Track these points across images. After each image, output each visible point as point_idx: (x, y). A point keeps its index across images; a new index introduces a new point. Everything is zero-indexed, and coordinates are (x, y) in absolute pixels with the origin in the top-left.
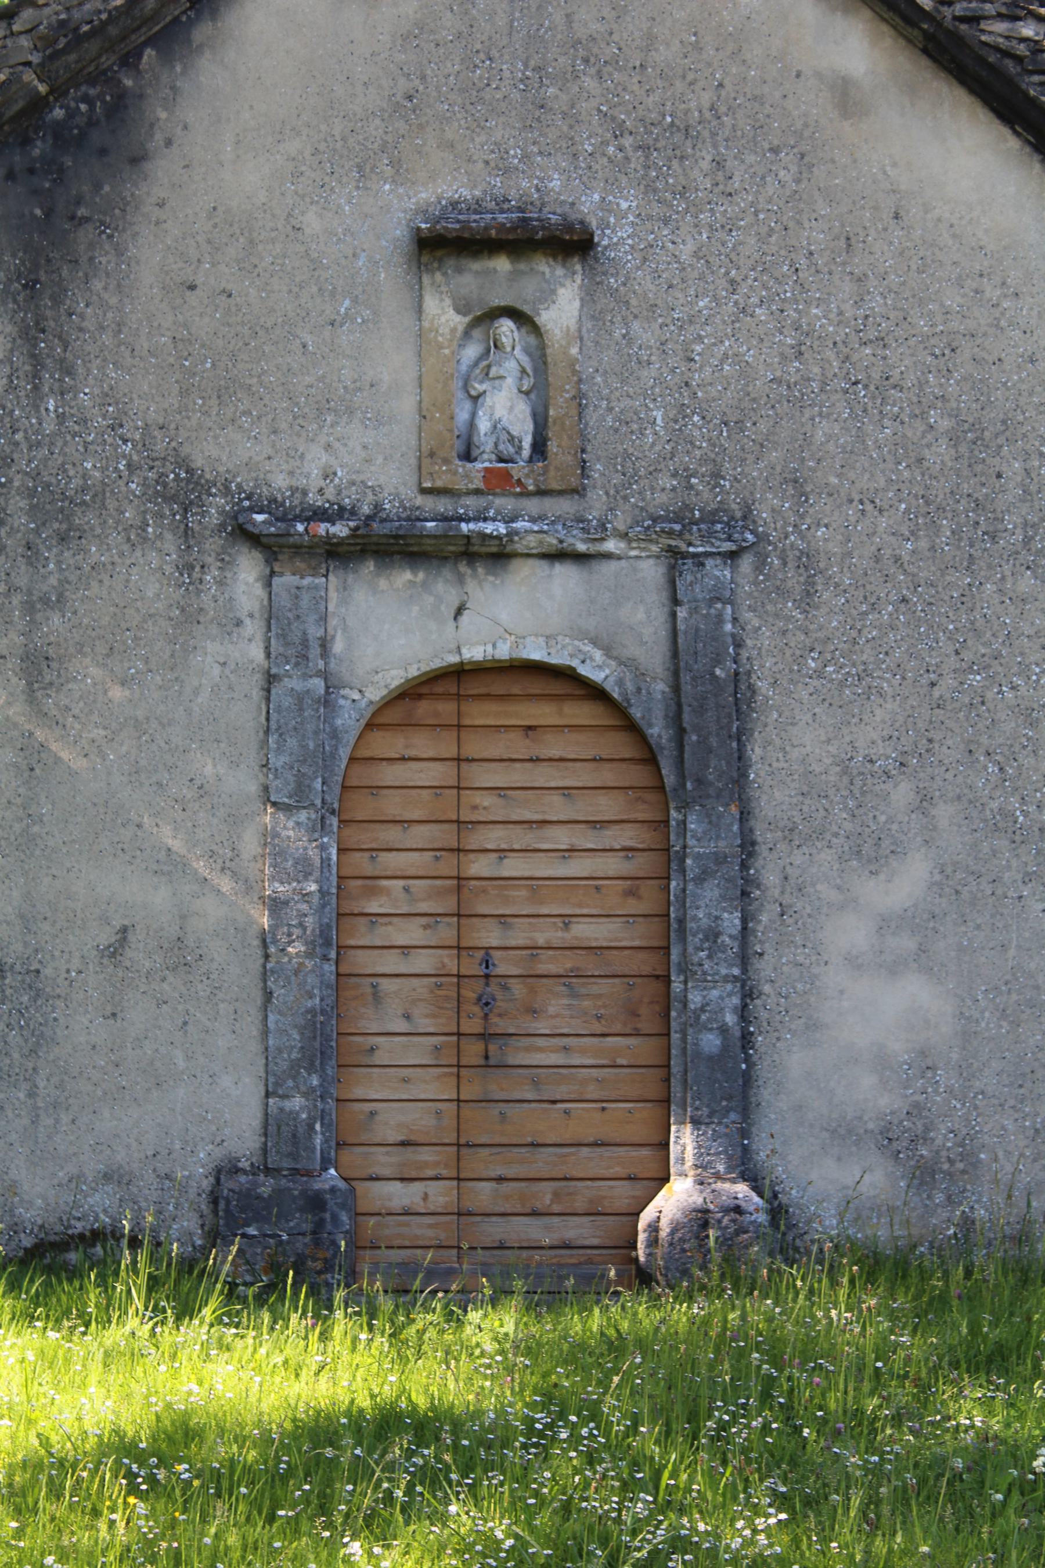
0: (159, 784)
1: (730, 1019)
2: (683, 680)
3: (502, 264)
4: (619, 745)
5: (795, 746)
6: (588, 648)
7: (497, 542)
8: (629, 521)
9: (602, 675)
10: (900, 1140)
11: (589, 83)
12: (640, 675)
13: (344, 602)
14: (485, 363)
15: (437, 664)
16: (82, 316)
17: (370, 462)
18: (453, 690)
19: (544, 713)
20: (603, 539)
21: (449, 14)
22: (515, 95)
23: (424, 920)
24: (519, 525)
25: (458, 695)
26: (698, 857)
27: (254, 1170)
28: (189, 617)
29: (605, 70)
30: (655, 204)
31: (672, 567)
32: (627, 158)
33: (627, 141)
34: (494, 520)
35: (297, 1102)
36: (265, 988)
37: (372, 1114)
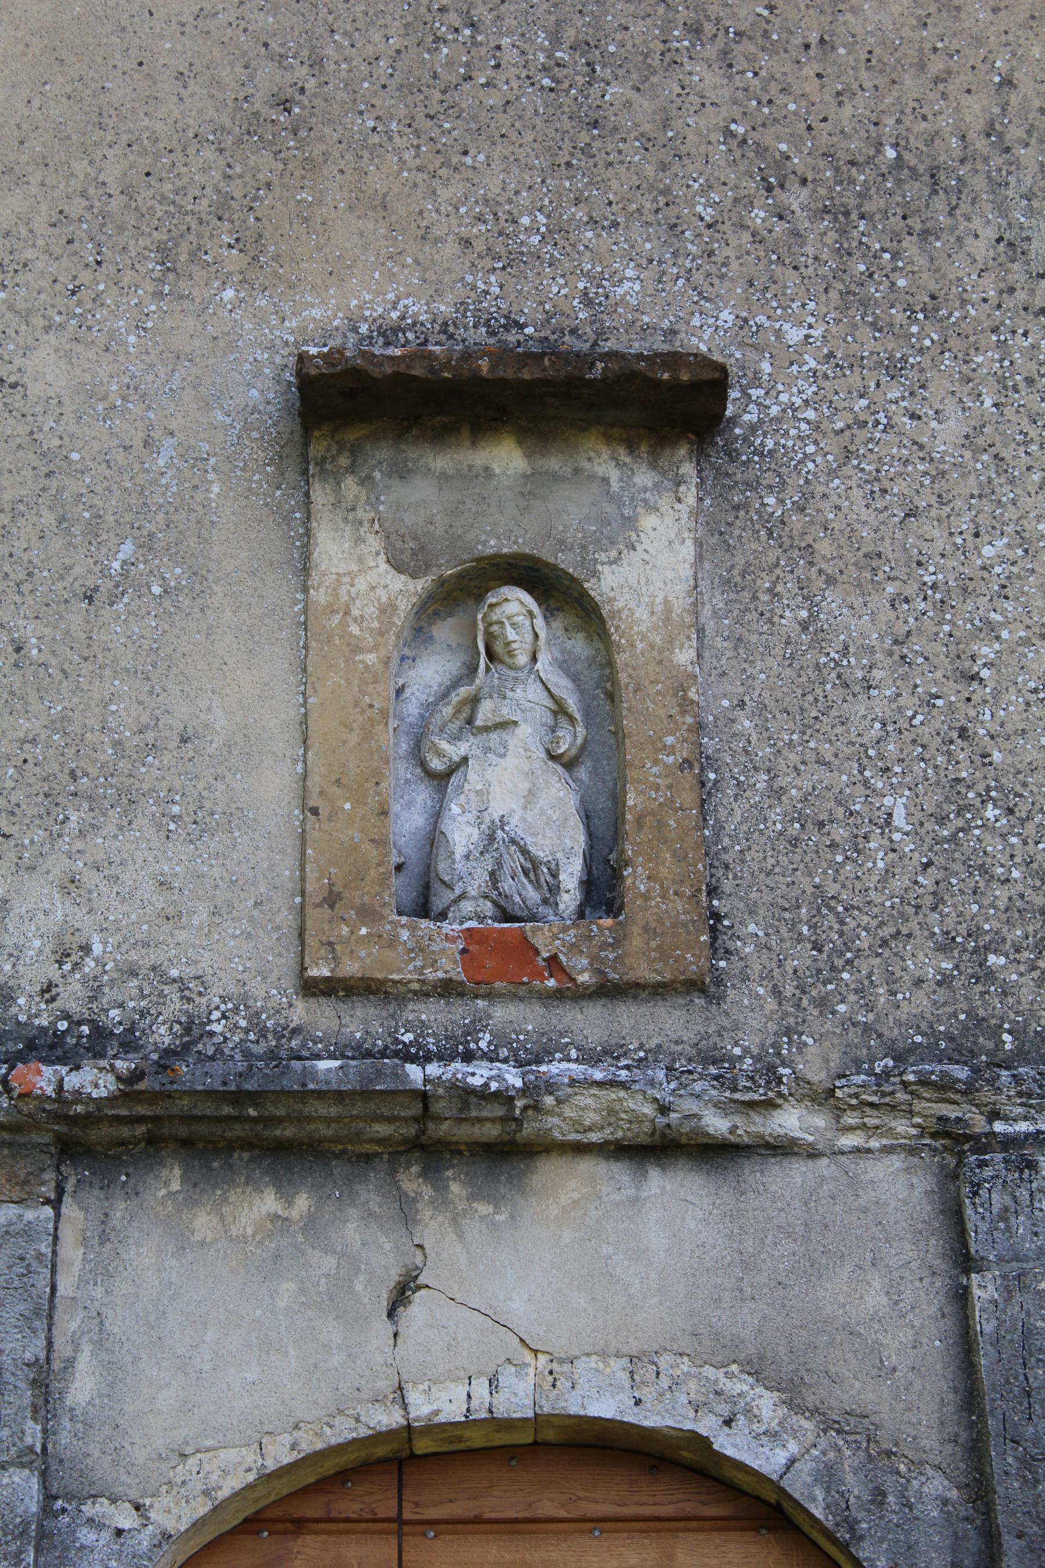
2: (997, 1465)
3: (505, 458)
6: (740, 1385)
7: (499, 1111)
8: (835, 1059)
9: (781, 1457)
11: (704, 76)
12: (880, 1455)
13: (101, 1271)
14: (464, 691)
15: (343, 1431)
18: (387, 1508)
20: (769, 1105)
22: (531, 99)
24: (553, 1068)
25: (399, 1520)
29: (738, 49)
30: (865, 333)
32: (796, 234)
33: (796, 198)
34: (491, 1057)
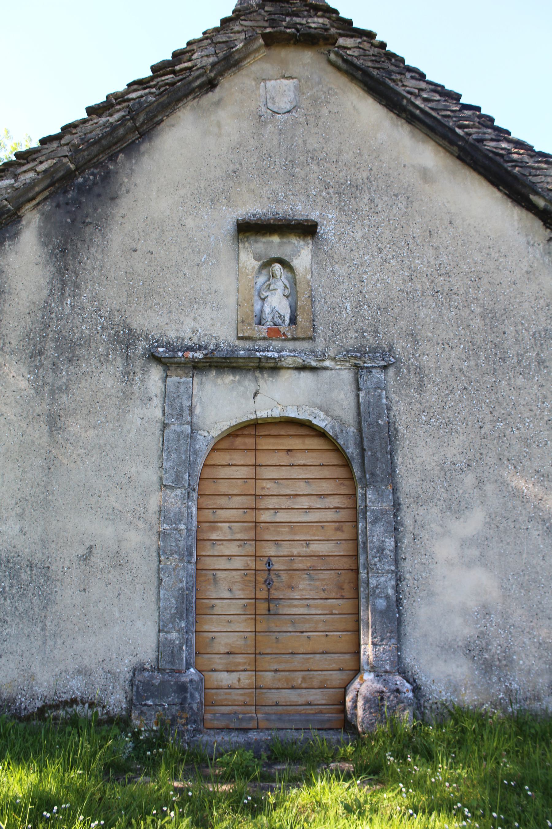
0: (110, 476)
1: (391, 592)
2: (363, 426)
3: (276, 239)
4: (331, 458)
5: (418, 456)
6: (317, 411)
7: (274, 361)
8: (336, 352)
9: (324, 424)
10: (486, 659)
11: (314, 167)
12: (342, 424)
13: (201, 390)
14: (268, 283)
15: (245, 419)
16: (85, 264)
17: (215, 326)
18: (253, 433)
19: (295, 443)
20: (323, 360)
21: (252, 140)
22: (281, 171)
23: (238, 543)
24: (284, 353)
25: (255, 435)
26: (373, 511)
27: (152, 670)
28: (127, 396)
29: (321, 162)
30: (344, 216)
31: (357, 374)
32: (331, 197)
33: (331, 191)
34: (272, 351)
35: (174, 635)
36: (159, 577)
37: (213, 638)
